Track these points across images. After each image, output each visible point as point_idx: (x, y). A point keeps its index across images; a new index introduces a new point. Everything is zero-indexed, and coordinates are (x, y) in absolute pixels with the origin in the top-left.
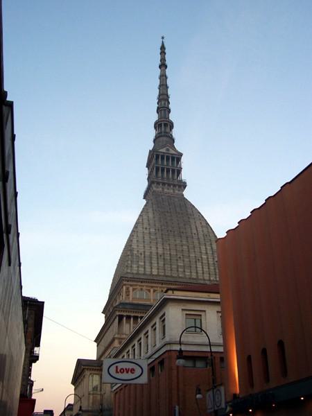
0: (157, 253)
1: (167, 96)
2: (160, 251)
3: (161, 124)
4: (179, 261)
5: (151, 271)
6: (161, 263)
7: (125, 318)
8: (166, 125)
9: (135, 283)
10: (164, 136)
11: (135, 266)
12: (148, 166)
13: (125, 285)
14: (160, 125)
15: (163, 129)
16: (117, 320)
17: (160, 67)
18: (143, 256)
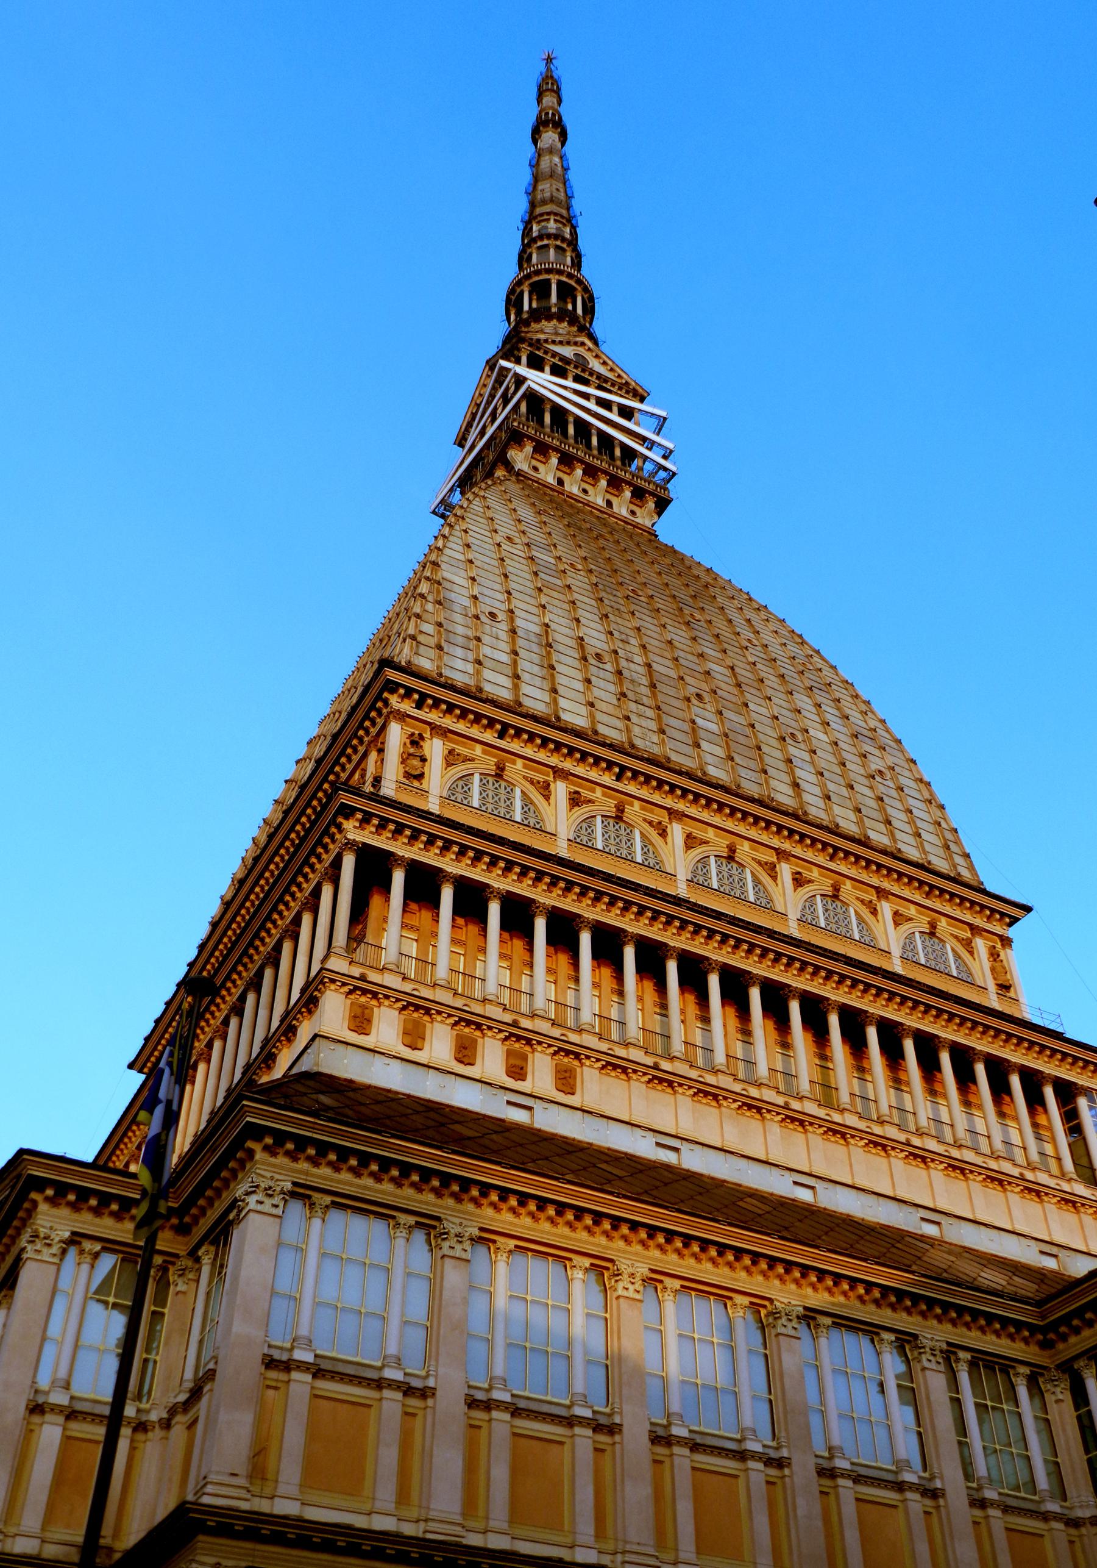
1: (568, 208)
2: (596, 640)
3: (548, 282)
4: (694, 709)
5: (555, 701)
6: (605, 690)
7: (398, 878)
9: (461, 727)
11: (459, 652)
13: (402, 717)
14: (541, 290)
16: (349, 862)
17: (536, 134)
18: (504, 626)
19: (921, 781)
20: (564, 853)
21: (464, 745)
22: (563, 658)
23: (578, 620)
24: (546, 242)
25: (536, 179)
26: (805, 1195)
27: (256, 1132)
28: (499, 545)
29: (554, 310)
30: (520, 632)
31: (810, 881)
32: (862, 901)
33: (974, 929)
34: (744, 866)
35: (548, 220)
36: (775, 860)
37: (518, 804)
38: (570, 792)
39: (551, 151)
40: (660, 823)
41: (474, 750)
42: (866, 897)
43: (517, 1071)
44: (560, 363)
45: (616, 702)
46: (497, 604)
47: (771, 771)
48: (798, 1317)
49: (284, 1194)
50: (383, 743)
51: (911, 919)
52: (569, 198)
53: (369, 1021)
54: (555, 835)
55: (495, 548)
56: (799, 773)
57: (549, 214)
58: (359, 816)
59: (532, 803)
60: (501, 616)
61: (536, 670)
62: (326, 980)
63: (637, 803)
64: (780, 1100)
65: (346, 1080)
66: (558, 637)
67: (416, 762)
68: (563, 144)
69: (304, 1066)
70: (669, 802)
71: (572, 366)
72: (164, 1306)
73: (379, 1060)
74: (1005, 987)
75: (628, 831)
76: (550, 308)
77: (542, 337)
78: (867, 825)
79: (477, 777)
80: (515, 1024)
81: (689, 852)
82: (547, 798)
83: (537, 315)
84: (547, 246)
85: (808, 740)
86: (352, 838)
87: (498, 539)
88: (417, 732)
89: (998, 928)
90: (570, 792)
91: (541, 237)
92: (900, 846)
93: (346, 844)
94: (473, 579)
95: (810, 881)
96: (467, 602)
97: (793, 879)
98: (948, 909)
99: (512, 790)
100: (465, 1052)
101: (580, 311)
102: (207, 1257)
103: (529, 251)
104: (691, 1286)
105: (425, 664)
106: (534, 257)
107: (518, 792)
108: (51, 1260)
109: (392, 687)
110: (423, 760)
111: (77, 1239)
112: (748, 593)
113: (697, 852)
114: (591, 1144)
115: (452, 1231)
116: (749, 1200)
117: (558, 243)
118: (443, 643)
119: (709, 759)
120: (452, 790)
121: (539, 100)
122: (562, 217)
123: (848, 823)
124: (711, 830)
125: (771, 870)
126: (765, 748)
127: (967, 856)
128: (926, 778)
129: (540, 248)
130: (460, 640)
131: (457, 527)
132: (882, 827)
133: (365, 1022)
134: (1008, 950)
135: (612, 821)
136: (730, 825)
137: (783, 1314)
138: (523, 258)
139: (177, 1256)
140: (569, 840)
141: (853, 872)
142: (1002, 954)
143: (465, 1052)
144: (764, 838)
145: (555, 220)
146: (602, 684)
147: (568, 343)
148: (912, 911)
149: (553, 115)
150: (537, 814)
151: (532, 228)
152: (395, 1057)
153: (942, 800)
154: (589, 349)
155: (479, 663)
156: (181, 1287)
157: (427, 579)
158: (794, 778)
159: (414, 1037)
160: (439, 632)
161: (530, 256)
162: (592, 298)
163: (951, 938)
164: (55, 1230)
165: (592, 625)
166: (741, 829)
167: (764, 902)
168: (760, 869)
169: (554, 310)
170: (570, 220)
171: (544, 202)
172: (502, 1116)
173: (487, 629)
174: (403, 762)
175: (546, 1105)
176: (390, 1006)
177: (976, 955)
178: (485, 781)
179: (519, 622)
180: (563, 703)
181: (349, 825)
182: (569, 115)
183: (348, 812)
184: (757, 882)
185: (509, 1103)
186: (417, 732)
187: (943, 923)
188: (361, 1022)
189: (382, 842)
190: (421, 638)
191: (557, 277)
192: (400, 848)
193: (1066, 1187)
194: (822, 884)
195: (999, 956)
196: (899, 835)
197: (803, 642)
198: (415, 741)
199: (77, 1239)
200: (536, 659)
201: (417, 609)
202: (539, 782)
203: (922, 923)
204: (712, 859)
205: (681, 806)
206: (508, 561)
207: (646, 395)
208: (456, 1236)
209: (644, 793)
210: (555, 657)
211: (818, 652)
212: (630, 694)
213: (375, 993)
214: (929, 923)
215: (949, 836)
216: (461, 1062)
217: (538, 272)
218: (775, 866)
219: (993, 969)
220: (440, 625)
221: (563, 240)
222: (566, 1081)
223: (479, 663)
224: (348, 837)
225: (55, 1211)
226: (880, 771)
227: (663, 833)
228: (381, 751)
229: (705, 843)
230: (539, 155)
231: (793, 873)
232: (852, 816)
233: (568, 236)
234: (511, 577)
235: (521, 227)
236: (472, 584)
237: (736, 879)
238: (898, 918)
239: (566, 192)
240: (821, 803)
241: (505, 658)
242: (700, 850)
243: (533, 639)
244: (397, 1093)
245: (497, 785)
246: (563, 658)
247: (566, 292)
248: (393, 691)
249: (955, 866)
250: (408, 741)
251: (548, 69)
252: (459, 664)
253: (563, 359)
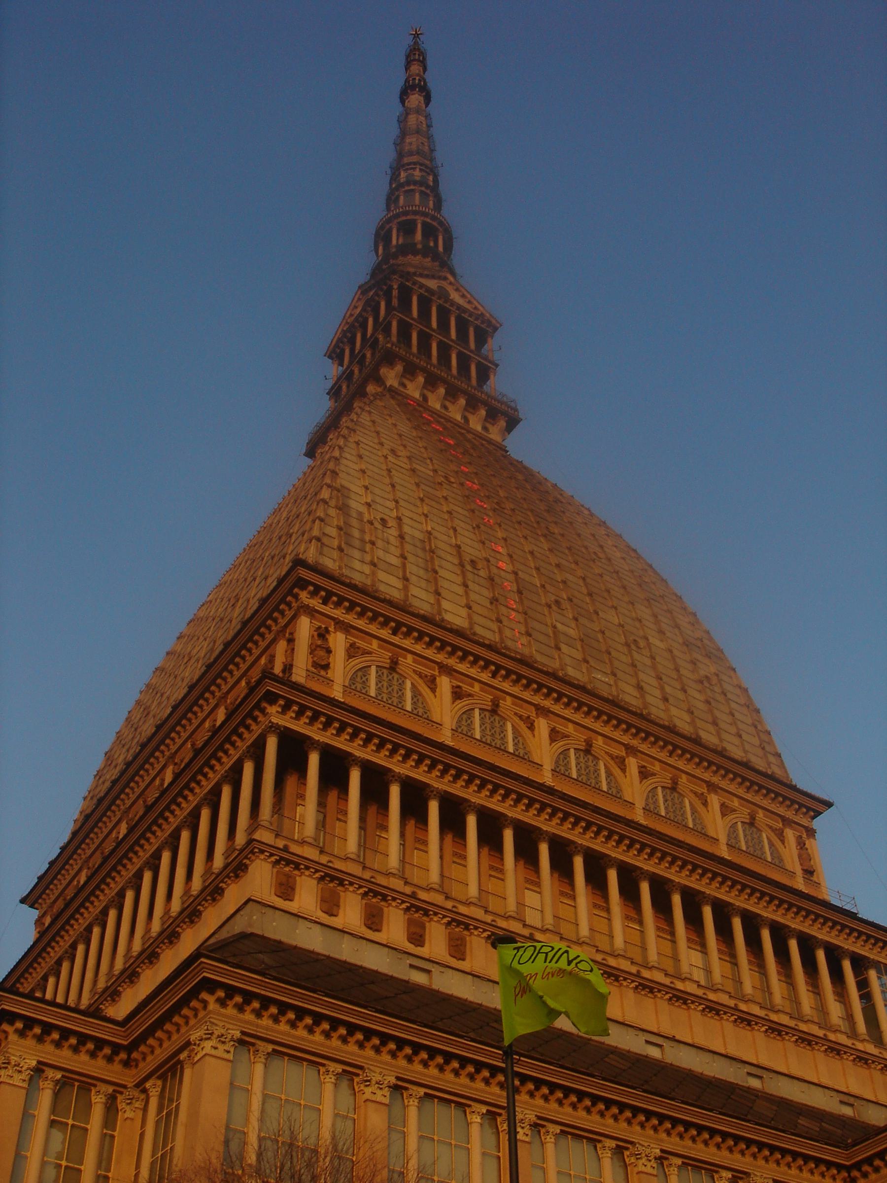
0: (458, 547)
1: (432, 160)
2: (472, 550)
3: (414, 222)
6: (481, 595)
9: (361, 623)
11: (357, 554)
12: (335, 354)
13: (311, 612)
14: (407, 229)
15: (419, 236)
16: (272, 744)
18: (394, 532)
19: (740, 687)
20: (449, 742)
21: (363, 640)
22: (444, 563)
23: (455, 530)
24: (412, 187)
25: (404, 133)
26: (654, 1053)
27: (210, 986)
28: (386, 457)
29: (419, 246)
30: (407, 538)
31: (653, 774)
32: (695, 793)
33: (786, 821)
34: (598, 759)
35: (414, 169)
36: (624, 754)
37: (409, 694)
38: (453, 686)
39: (418, 111)
40: (529, 717)
41: (371, 644)
42: (700, 790)
43: (417, 938)
44: (426, 294)
45: (488, 605)
46: (387, 511)
47: (620, 674)
48: (655, 1158)
49: (234, 1041)
50: (291, 634)
51: (735, 810)
52: (432, 150)
53: (293, 889)
54: (441, 725)
55: (382, 459)
56: (642, 676)
57: (415, 163)
58: (282, 702)
59: (421, 694)
60: (391, 523)
61: (422, 573)
62: (256, 850)
63: (508, 698)
64: (634, 969)
65: (275, 941)
66: (441, 545)
67: (322, 653)
68: (427, 105)
69: (239, 926)
70: (537, 699)
71: (436, 296)
72: (114, 1130)
73: (303, 924)
74: (809, 872)
75: (501, 723)
76: (415, 244)
77: (412, 270)
78: (698, 725)
79: (373, 668)
80: (413, 896)
81: (553, 744)
82: (433, 690)
83: (407, 249)
84: (412, 190)
85: (649, 645)
86: (275, 722)
87: (385, 452)
88: (323, 626)
89: (804, 822)
90: (453, 686)
91: (408, 183)
92: (726, 745)
93: (271, 727)
94: (366, 488)
95: (653, 774)
96: (363, 509)
97: (639, 772)
98: (765, 803)
99: (403, 681)
100: (373, 920)
101: (441, 249)
102: (154, 1090)
103: (397, 193)
104: (571, 1132)
105: (330, 563)
106: (402, 198)
107: (408, 684)
108: (21, 1084)
109: (302, 584)
110: (329, 651)
111: (42, 1067)
112: (589, 510)
113: (560, 745)
114: (481, 1005)
115: (374, 1079)
116: (611, 1056)
117: (423, 189)
118: (343, 545)
119: (568, 660)
120: (353, 679)
121: (407, 68)
122: (426, 167)
123: (683, 723)
124: (570, 725)
125: (621, 764)
126: (614, 653)
127: (779, 755)
128: (745, 684)
129: (406, 192)
130: (357, 543)
131: (350, 439)
132: (711, 728)
133: (290, 889)
134: (812, 840)
135: (487, 714)
136: (588, 722)
137: (644, 1155)
138: (391, 199)
139: (125, 1087)
140: (452, 729)
141: (689, 768)
142: (807, 842)
143: (373, 920)
144: (617, 735)
145: (420, 169)
146: (477, 588)
147: (433, 277)
148: (736, 803)
149: (419, 80)
150: (425, 705)
151: (399, 174)
152: (316, 922)
153: (758, 705)
154: (451, 283)
155: (375, 565)
156: (130, 1114)
157: (329, 486)
158: (638, 681)
159: (331, 905)
160: (340, 535)
161: (398, 198)
163: (767, 828)
164: (24, 1059)
165: (466, 533)
166: (598, 726)
167: (614, 791)
168: (612, 762)
169: (419, 246)
170: (432, 170)
171: (411, 153)
172: (406, 978)
173: (380, 534)
174: (312, 652)
175: (442, 969)
176: (310, 876)
177: (786, 844)
178: (380, 673)
179: (406, 529)
180: (445, 605)
181: (273, 710)
182: (432, 79)
183: (271, 698)
184: (609, 774)
185: (411, 966)
186: (323, 626)
187: (760, 814)
188: (286, 890)
189: (300, 727)
190: (325, 540)
191: (422, 218)
192: (315, 733)
193: (860, 1046)
194: (663, 777)
195: (805, 844)
196: (725, 736)
197: (639, 557)
198: (322, 634)
199: (42, 1067)
200: (421, 562)
201: (320, 513)
202: (426, 676)
203: (744, 813)
204: (572, 751)
205: (547, 703)
206: (394, 472)
207: (498, 325)
208: (377, 1083)
209: (516, 690)
210: (437, 562)
211: (651, 566)
212: (502, 600)
213: (297, 864)
214: (749, 814)
215: (764, 737)
216: (370, 928)
217: (406, 213)
218: (624, 760)
219: (800, 856)
220: (340, 529)
221: (428, 187)
222: (458, 949)
223: (375, 565)
224: (272, 720)
225: (22, 1041)
226: (707, 677)
227: (531, 727)
228: (291, 641)
229: (566, 737)
230: (407, 114)
231: (639, 766)
232: (687, 717)
233: (431, 184)
234: (398, 487)
235: (389, 172)
236: (366, 492)
237: (592, 769)
238: (725, 810)
239: (429, 146)
240: (661, 705)
241: (395, 561)
242: (561, 743)
243: (419, 544)
244: (319, 954)
245: (390, 677)
246: (444, 563)
247: (429, 232)
248: (303, 588)
249: (769, 764)
250: (316, 633)
251: (416, 43)
252: (357, 565)
253: (428, 290)
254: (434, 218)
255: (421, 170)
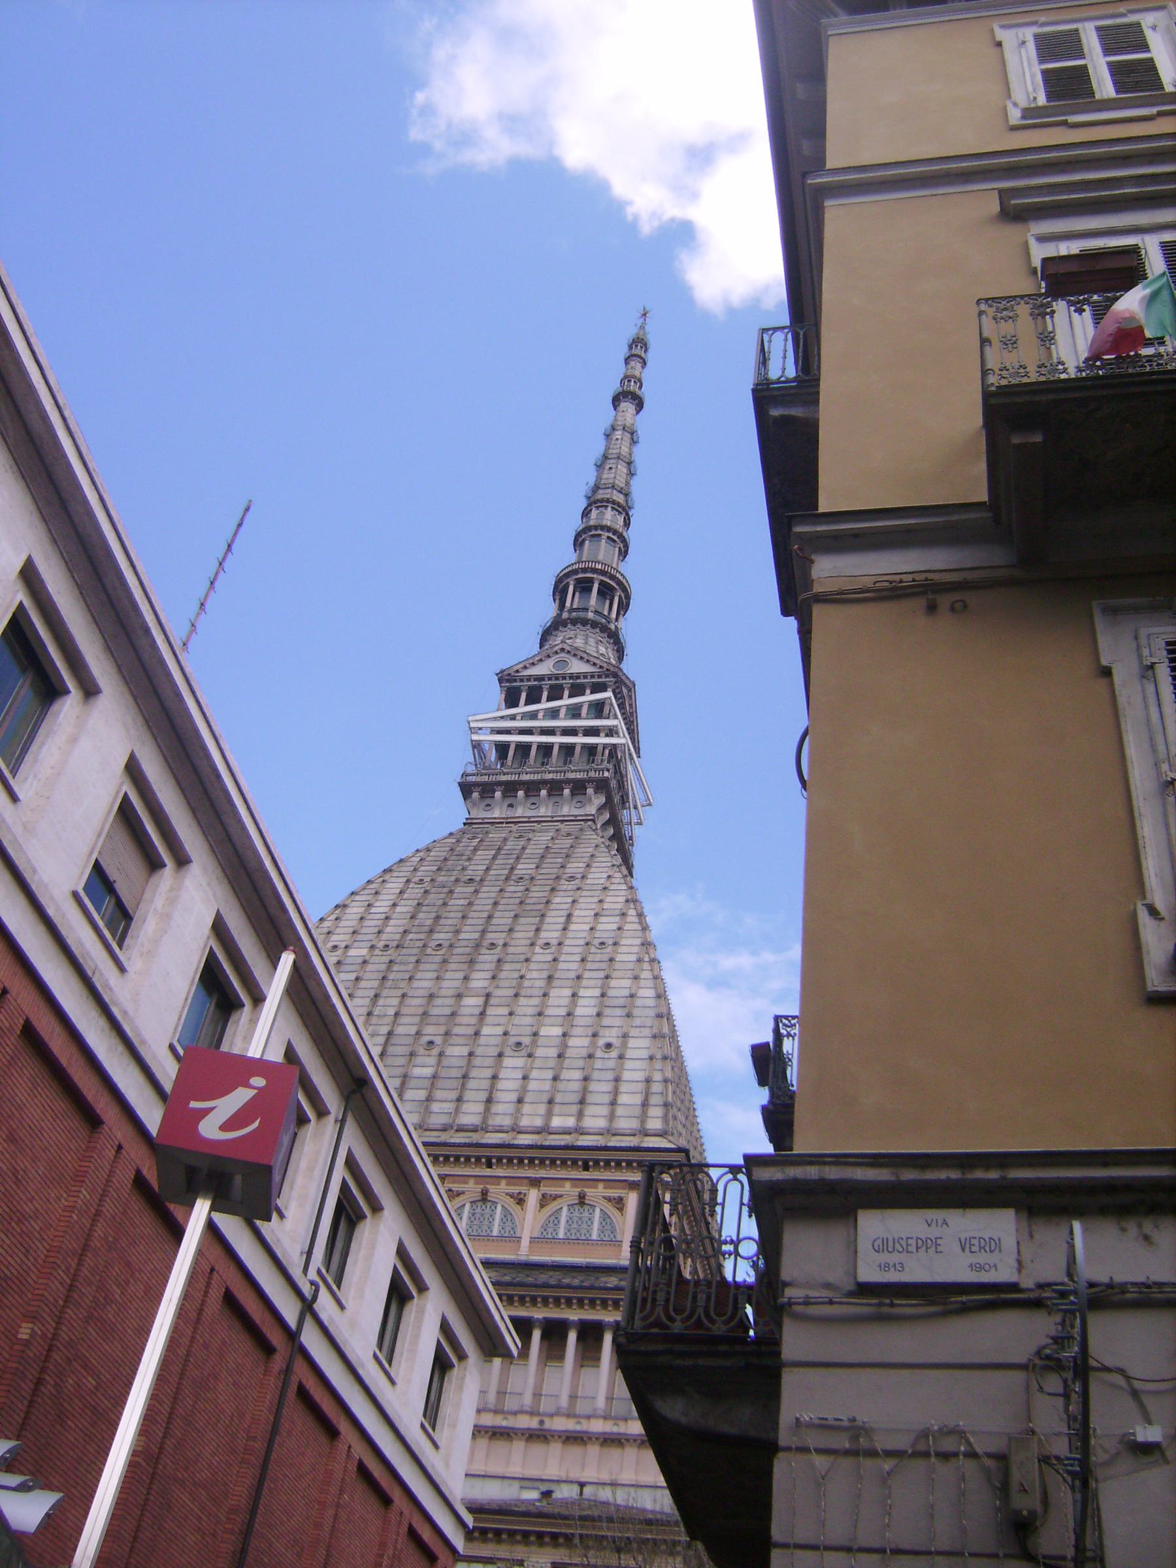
3: (591, 581)
8: (606, 592)
10: (594, 624)
14: (584, 587)
17: (616, 401)
24: (599, 532)
35: (607, 506)
57: (608, 501)
84: (600, 535)
101: (614, 615)
106: (587, 542)
117: (611, 535)
122: (619, 504)
129: (593, 536)
162: (628, 597)
217: (584, 570)
221: (615, 532)
251: (642, 327)
254: (613, 577)
255: (613, 509)
